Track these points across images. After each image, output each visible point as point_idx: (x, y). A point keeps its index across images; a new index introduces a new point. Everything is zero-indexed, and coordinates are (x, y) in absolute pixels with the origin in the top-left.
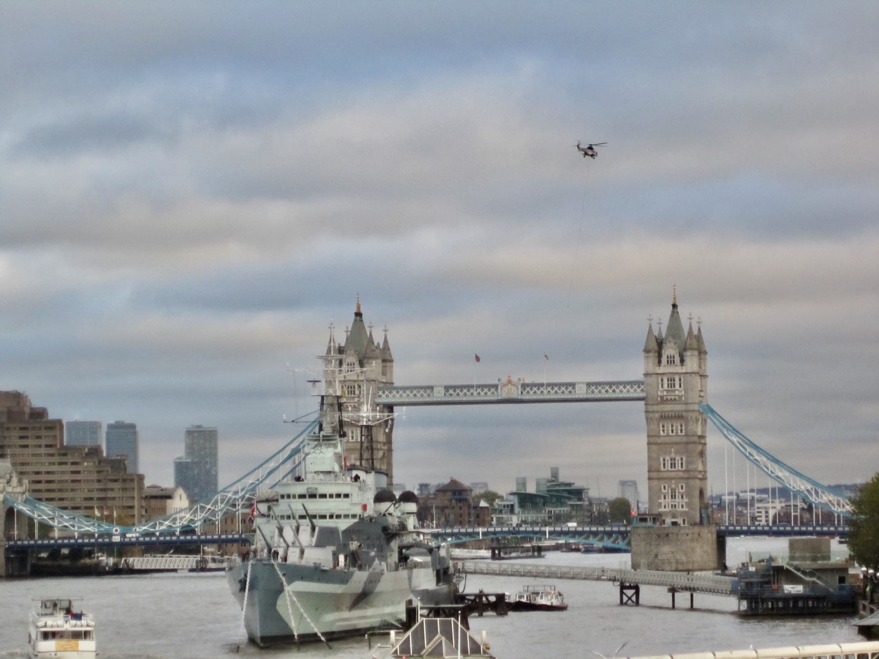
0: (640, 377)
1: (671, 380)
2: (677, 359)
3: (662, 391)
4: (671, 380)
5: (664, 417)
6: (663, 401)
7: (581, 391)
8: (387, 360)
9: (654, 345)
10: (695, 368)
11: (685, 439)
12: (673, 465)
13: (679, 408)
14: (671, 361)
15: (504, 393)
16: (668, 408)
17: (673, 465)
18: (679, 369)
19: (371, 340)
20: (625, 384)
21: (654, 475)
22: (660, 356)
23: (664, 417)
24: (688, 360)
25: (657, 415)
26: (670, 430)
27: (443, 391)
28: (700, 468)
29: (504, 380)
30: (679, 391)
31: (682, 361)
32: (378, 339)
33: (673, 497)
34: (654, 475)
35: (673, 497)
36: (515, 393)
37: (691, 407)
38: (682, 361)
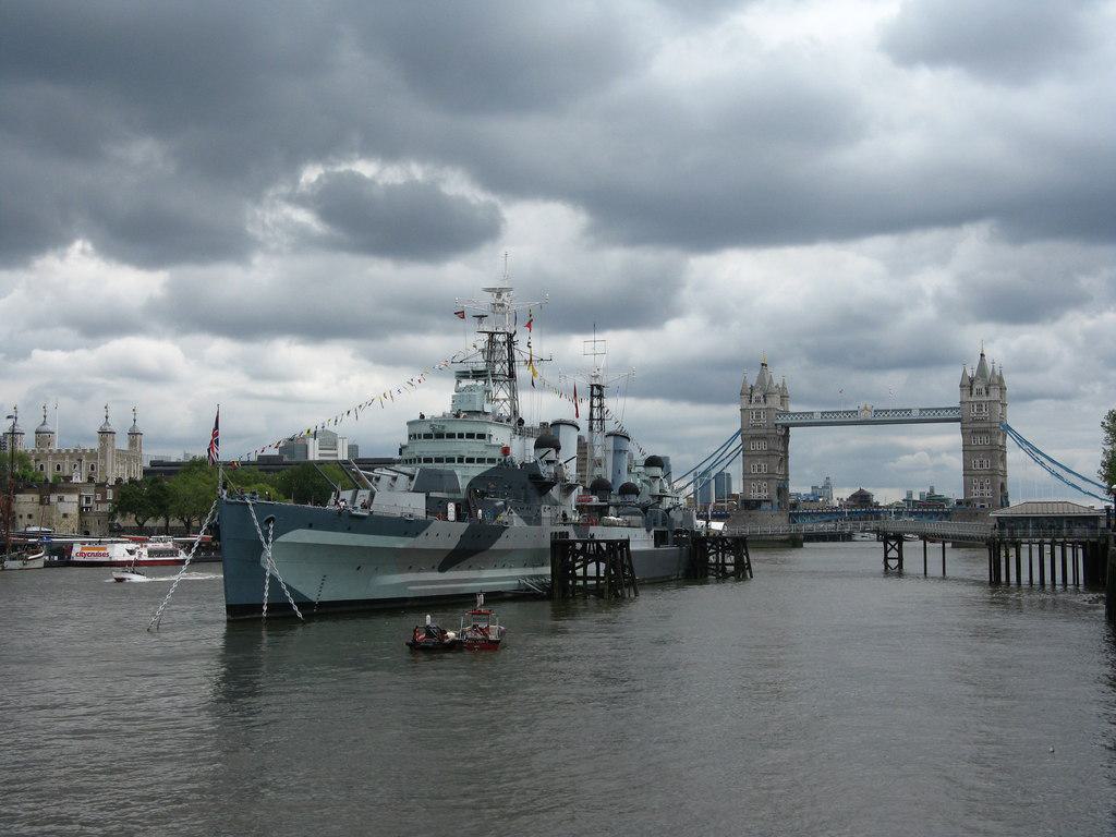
0: (957, 405)
1: (980, 405)
2: (984, 392)
3: (973, 414)
4: (980, 405)
5: (974, 432)
6: (975, 421)
7: (915, 415)
8: (784, 398)
9: (967, 382)
10: (997, 397)
11: (989, 448)
12: (981, 466)
13: (985, 425)
14: (979, 393)
15: (862, 416)
16: (977, 425)
17: (981, 466)
18: (985, 399)
19: (771, 381)
20: (947, 409)
21: (968, 472)
22: (971, 389)
23: (974, 432)
24: (991, 392)
25: (970, 431)
26: (981, 441)
27: (820, 415)
28: (1001, 468)
29: (862, 407)
30: (985, 413)
31: (987, 393)
32: (777, 381)
33: (982, 488)
34: (968, 472)
35: (982, 488)
36: (870, 416)
37: (993, 425)
38: (987, 393)
